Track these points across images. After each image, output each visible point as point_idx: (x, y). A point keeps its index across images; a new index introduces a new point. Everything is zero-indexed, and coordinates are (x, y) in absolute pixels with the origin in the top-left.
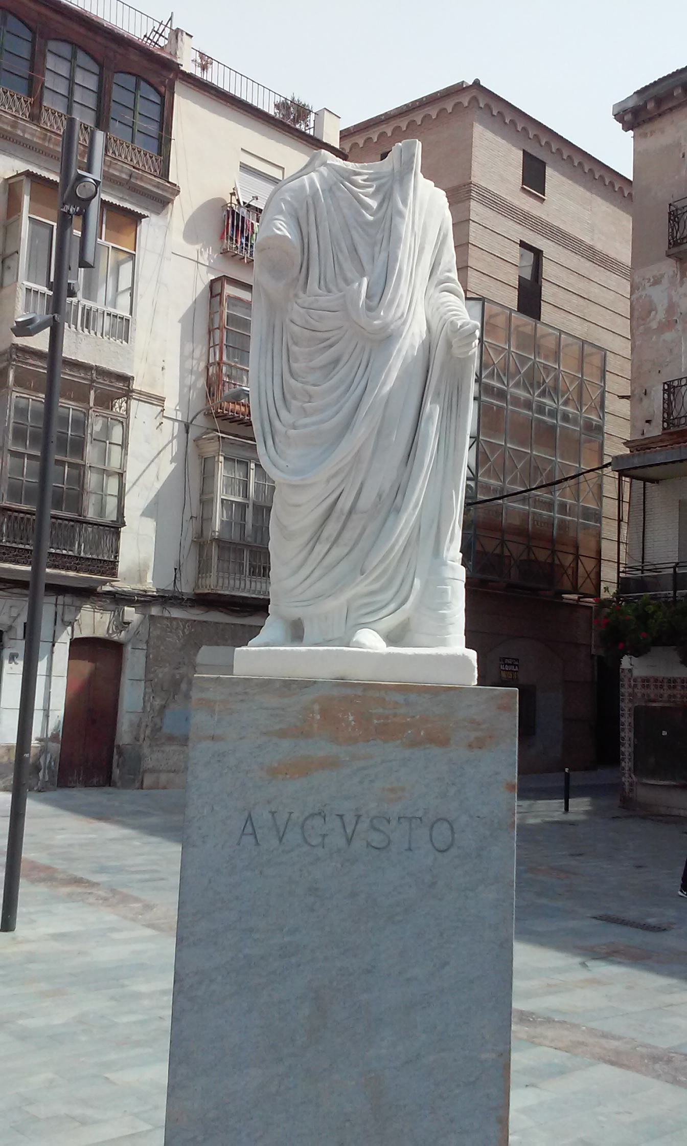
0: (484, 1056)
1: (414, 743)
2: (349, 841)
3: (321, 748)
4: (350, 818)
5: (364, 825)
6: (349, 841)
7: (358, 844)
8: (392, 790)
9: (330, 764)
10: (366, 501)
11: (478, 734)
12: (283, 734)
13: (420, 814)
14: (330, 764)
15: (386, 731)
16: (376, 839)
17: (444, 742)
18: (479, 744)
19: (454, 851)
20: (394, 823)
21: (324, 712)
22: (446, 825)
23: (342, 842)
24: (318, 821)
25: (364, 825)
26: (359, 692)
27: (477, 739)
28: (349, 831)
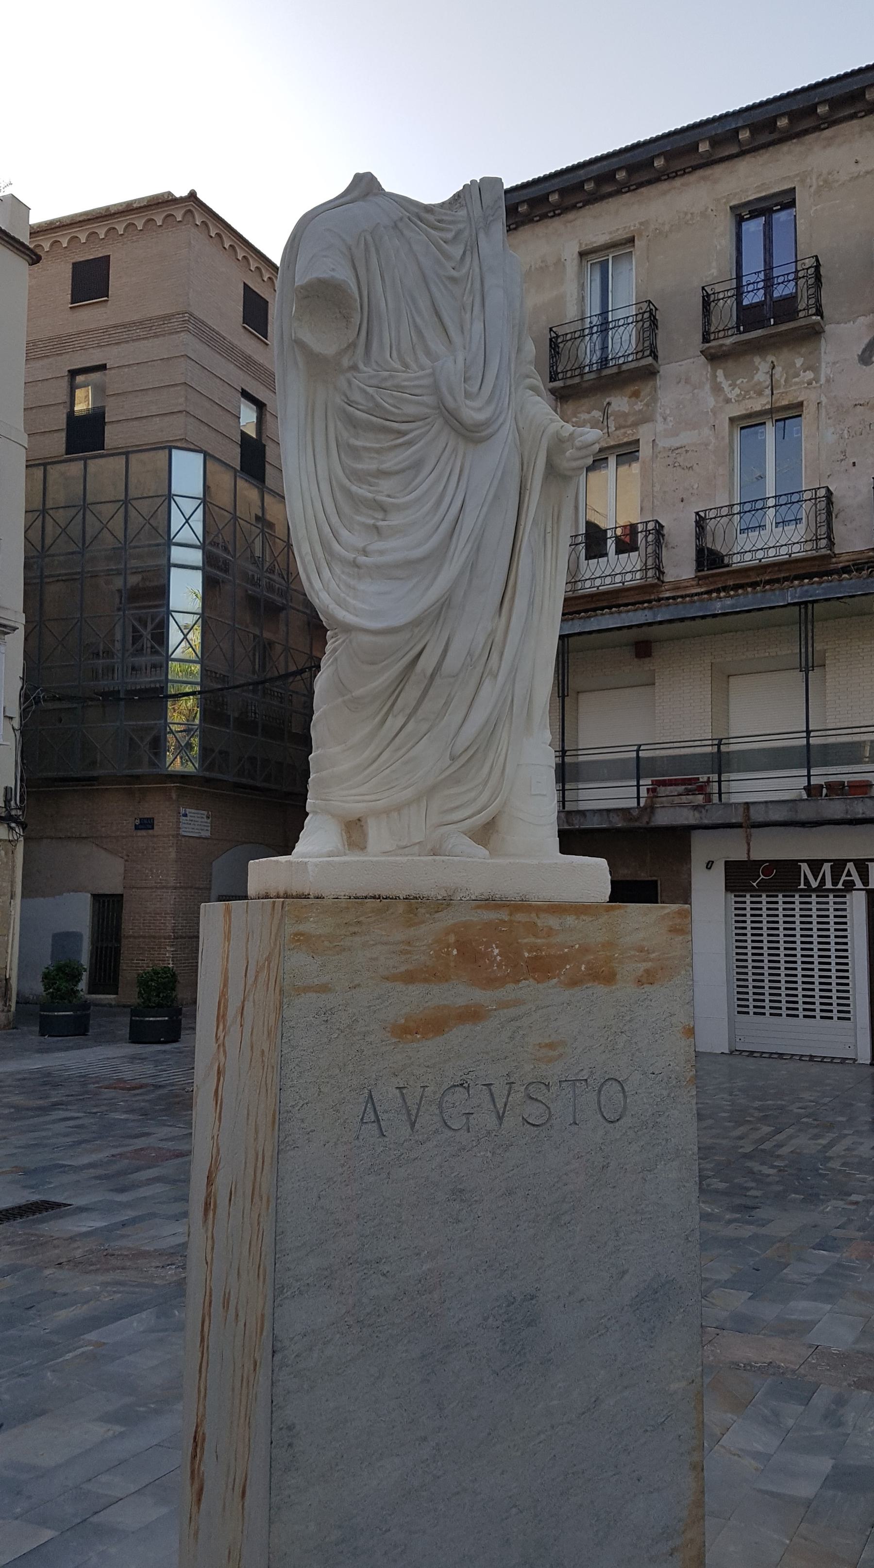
0: (674, 1386)
1: (574, 983)
2: (500, 1118)
3: (460, 993)
4: (499, 1089)
5: (518, 1096)
6: (500, 1118)
7: (510, 1122)
8: (551, 1046)
9: (473, 1015)
10: (452, 662)
11: (649, 965)
12: (409, 978)
13: (585, 1075)
14: (473, 1015)
15: (541, 967)
16: (534, 1112)
17: (609, 978)
18: (647, 979)
19: (626, 1121)
20: (553, 1089)
21: (461, 945)
22: (615, 1084)
23: (491, 1121)
24: (460, 1093)
25: (518, 1096)
26: (504, 915)
27: (647, 971)
28: (500, 1106)
